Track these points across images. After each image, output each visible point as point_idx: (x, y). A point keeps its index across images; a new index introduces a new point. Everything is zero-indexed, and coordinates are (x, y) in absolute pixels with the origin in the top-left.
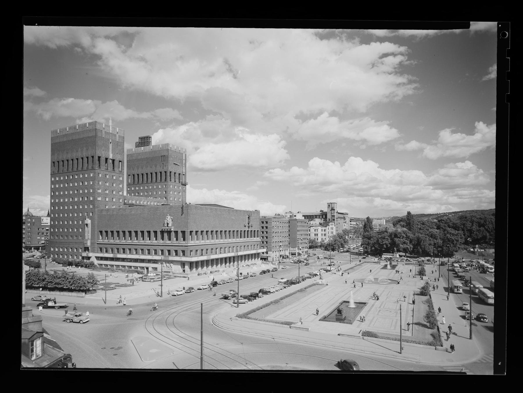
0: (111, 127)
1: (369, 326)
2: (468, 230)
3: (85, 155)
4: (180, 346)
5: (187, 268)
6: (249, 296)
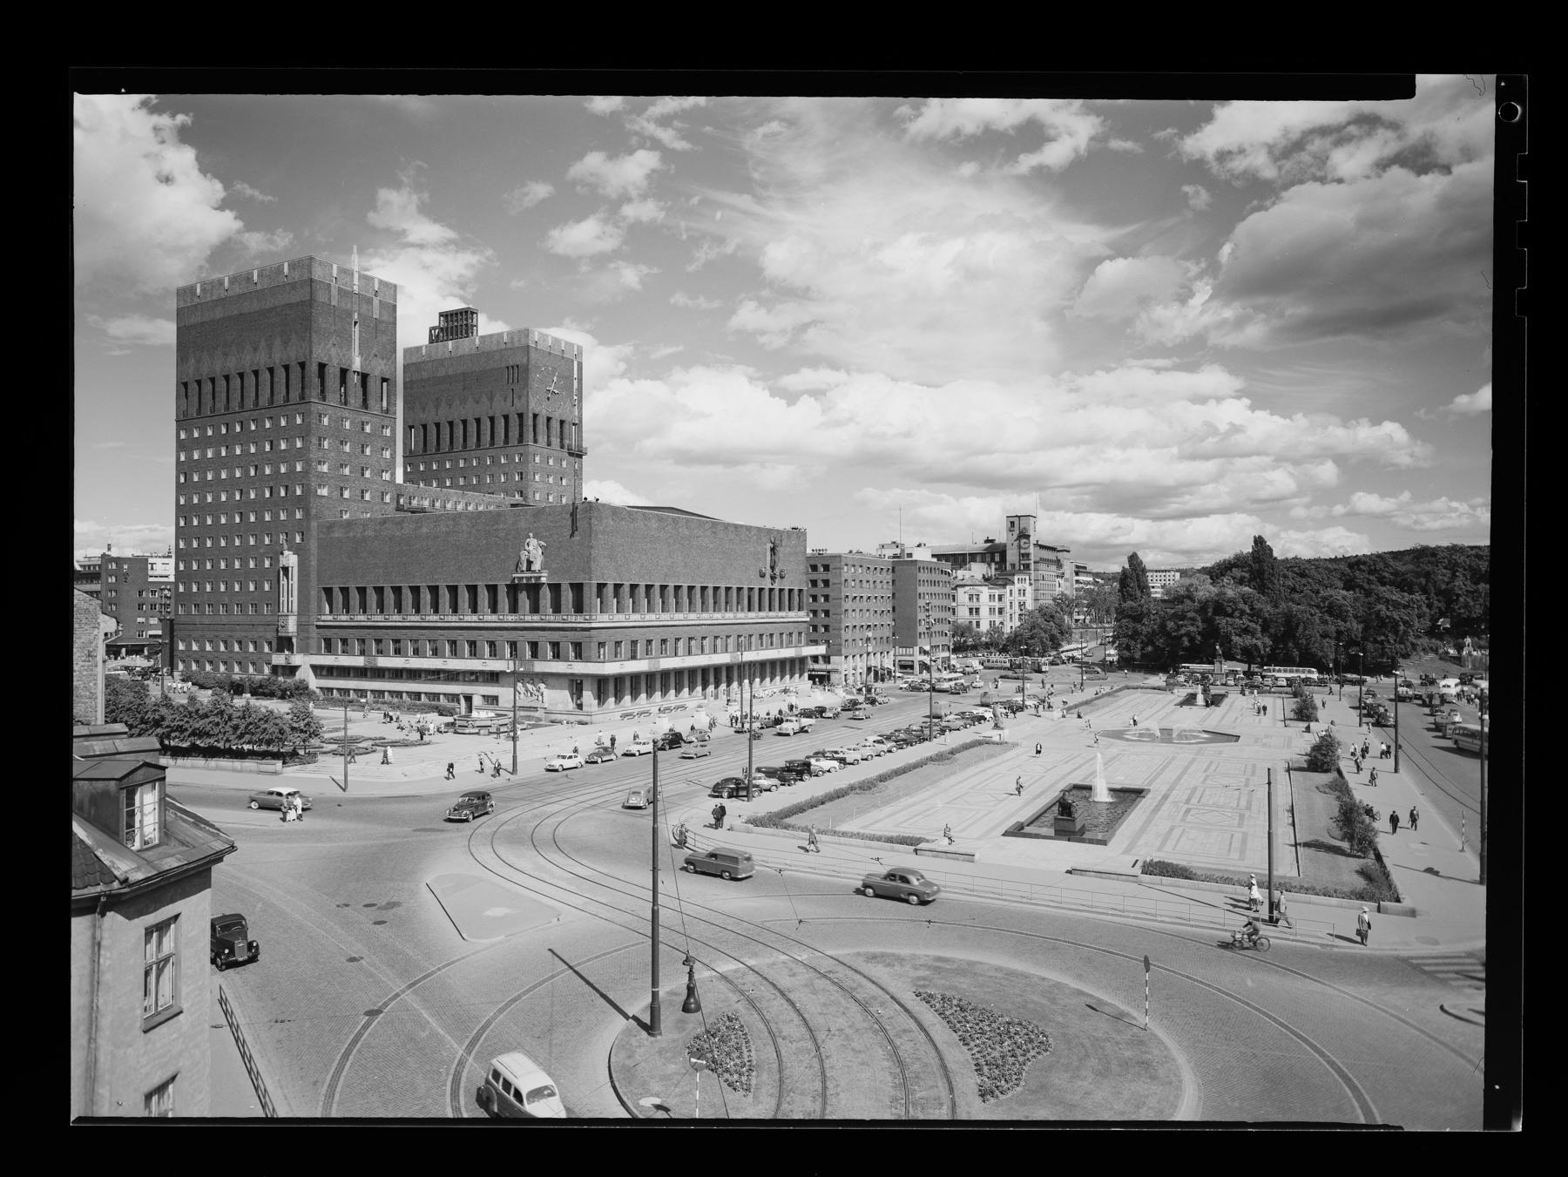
0: (356, 276)
1: (1159, 850)
2: (1439, 593)
3: (278, 358)
4: (579, 901)
5: (588, 696)
6: (783, 770)
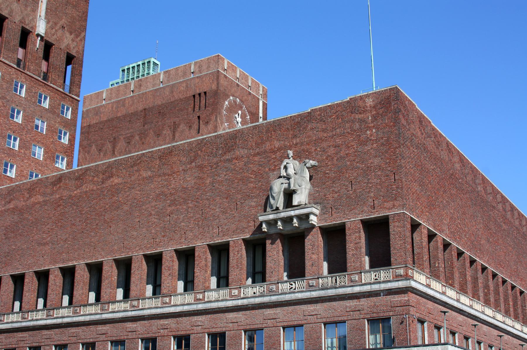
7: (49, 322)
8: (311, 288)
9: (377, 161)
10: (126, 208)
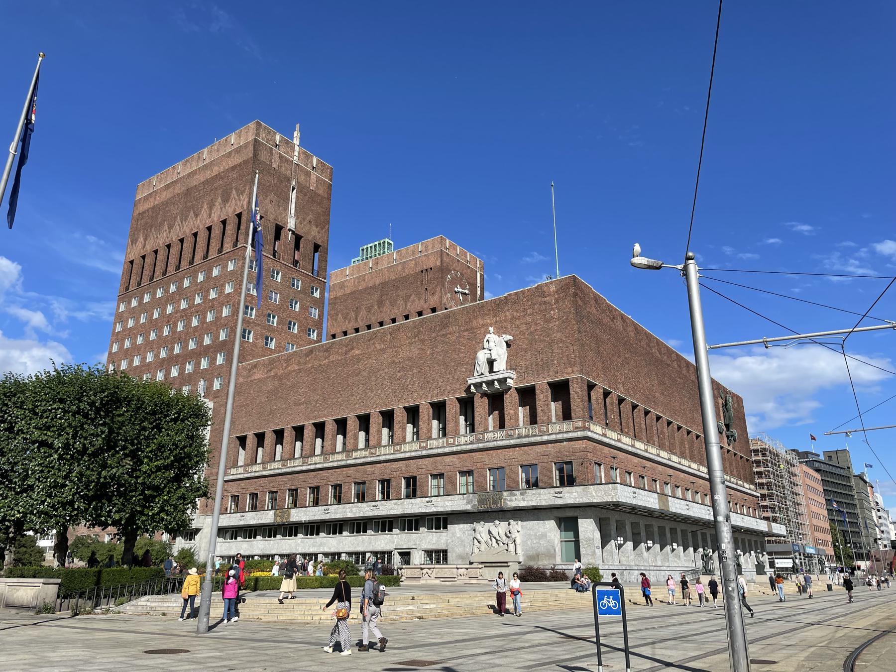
0: (297, 148)
3: (217, 216)
7: (304, 468)
8: (509, 437)
9: (559, 335)
10: (365, 374)
